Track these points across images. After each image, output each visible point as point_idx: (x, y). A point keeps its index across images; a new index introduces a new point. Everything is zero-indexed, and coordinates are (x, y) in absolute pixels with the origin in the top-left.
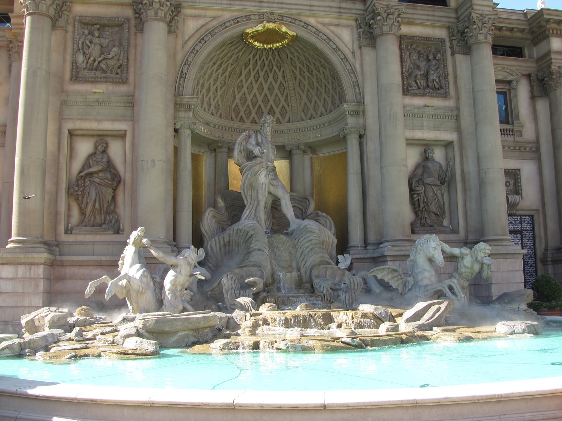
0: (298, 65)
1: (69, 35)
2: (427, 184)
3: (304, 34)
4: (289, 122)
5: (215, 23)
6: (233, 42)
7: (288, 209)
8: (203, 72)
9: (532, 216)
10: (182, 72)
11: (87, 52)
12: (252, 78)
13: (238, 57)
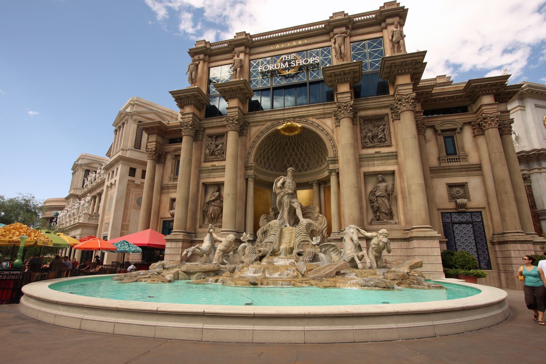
0: (311, 141)
2: (378, 196)
5: (264, 127)
7: (299, 213)
9: (481, 212)
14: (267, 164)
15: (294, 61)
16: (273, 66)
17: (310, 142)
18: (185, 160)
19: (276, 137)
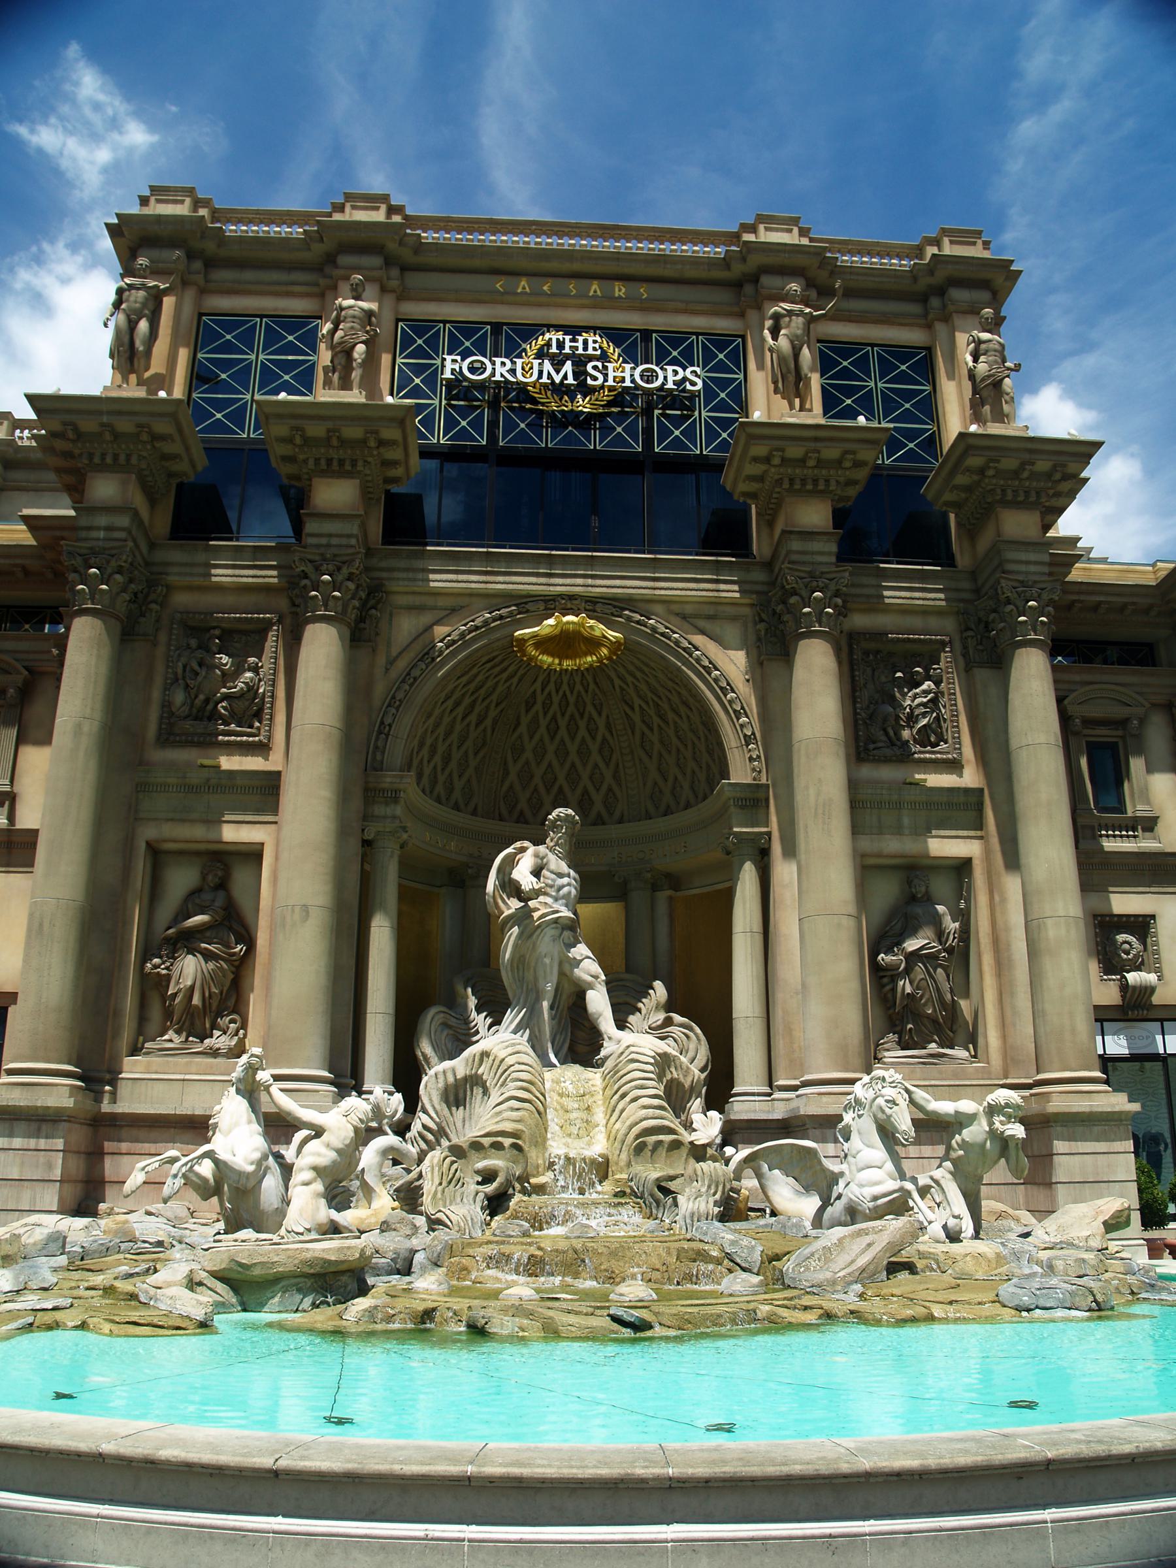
1: (161, 651)
4: (621, 821)
6: (494, 658)
8: (431, 721)
10: (382, 723)
11: (192, 683)
12: (543, 730)
13: (509, 688)
15: (599, 364)
16: (509, 365)
17: (632, 709)
18: (86, 728)
19: (497, 669)
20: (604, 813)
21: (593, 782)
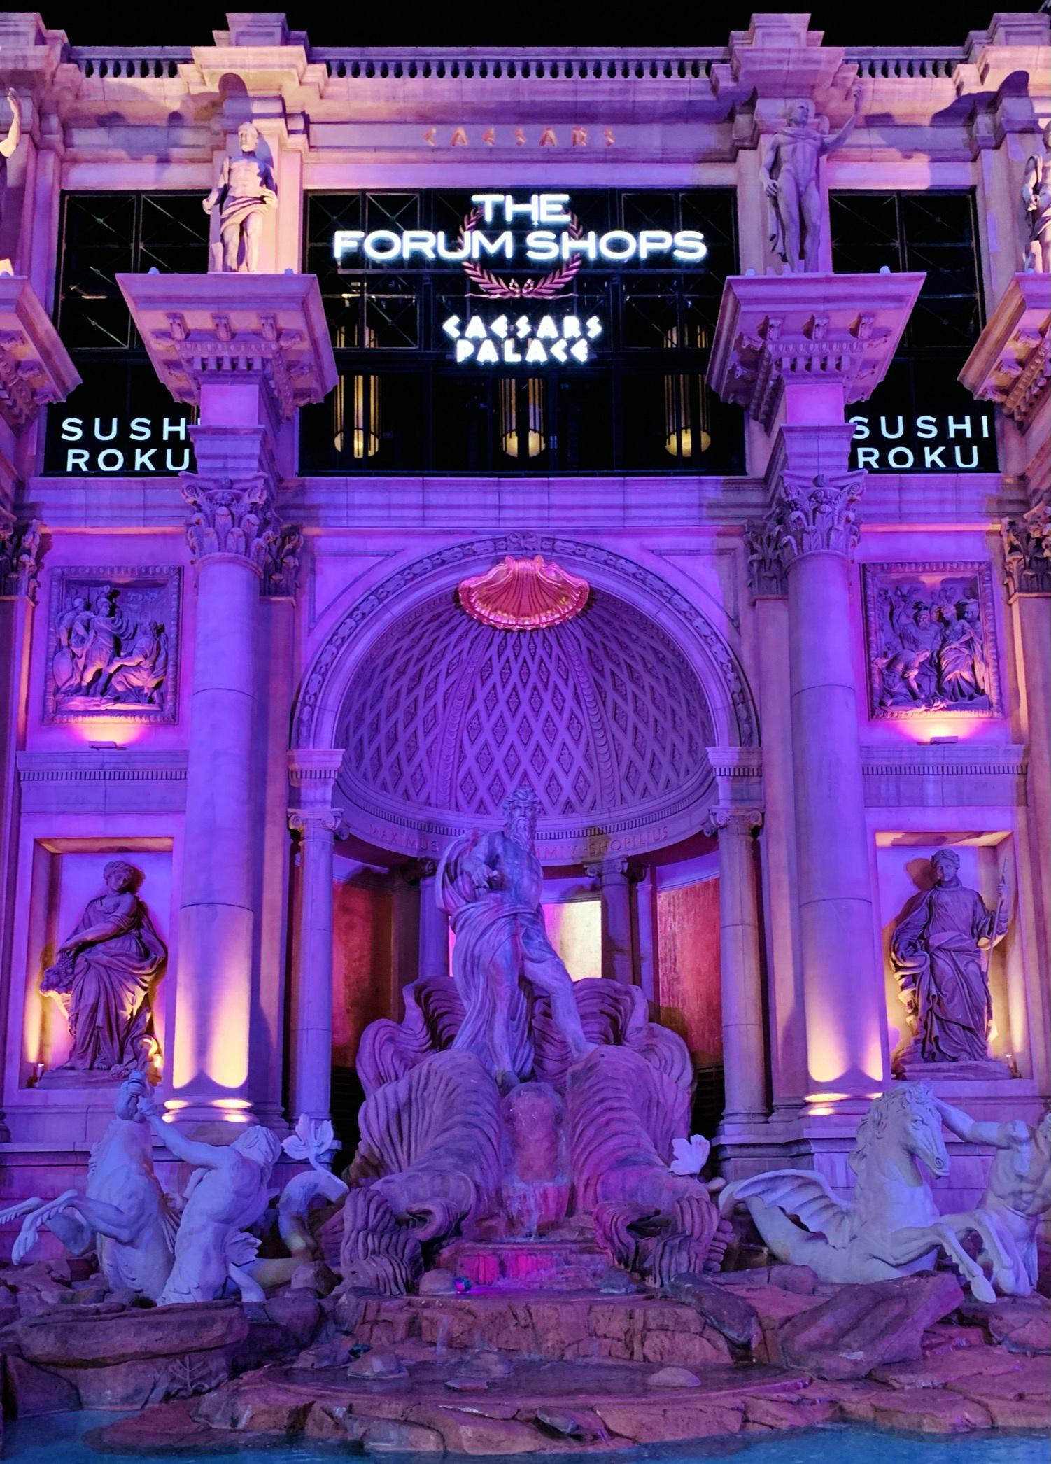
3: (609, 584)
5: (390, 568)
6: (439, 615)
12: (502, 707)
14: (387, 762)
20: (574, 798)
21: (561, 765)
